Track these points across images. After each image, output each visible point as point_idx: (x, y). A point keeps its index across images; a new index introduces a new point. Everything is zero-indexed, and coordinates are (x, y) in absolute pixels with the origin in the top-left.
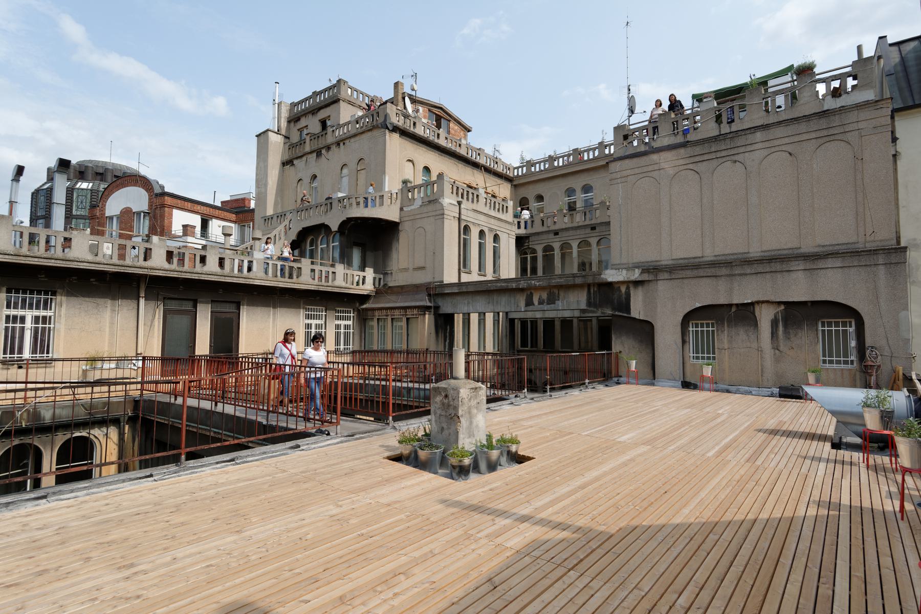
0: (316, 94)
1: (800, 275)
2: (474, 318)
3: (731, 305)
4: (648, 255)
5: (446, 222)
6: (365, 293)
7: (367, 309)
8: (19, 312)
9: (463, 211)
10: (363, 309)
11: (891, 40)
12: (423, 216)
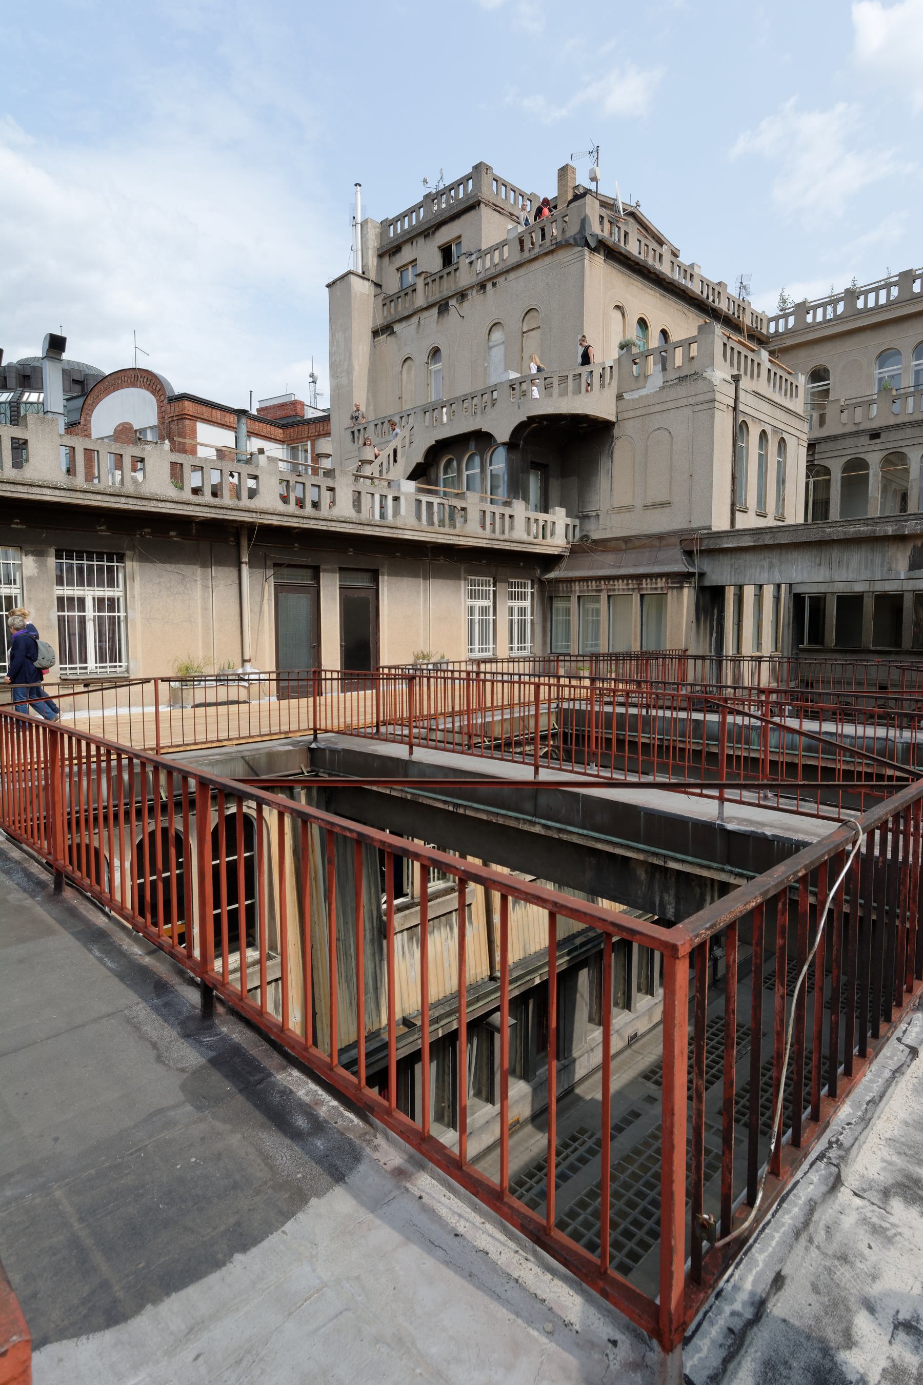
2: (749, 592)
5: (717, 413)
6: (555, 551)
7: (557, 581)
8: (75, 591)
9: (742, 394)
10: (550, 581)
12: (666, 406)
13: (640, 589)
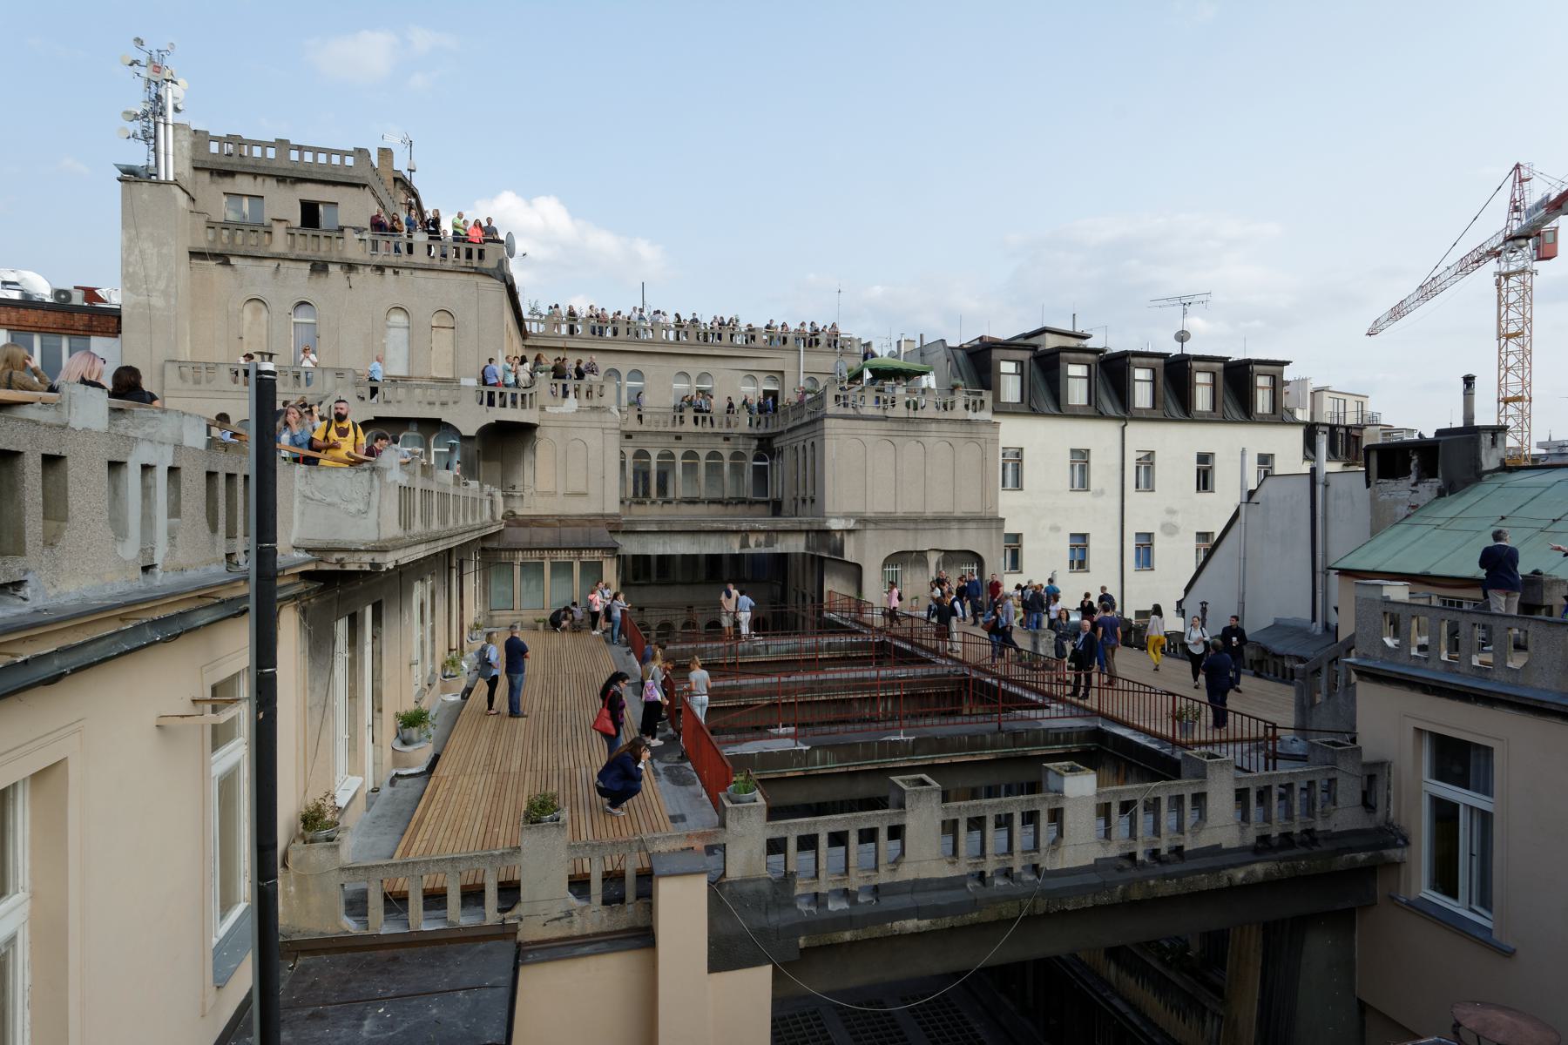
0: (282, 145)
1: (955, 532)
4: (857, 507)
11: (949, 344)
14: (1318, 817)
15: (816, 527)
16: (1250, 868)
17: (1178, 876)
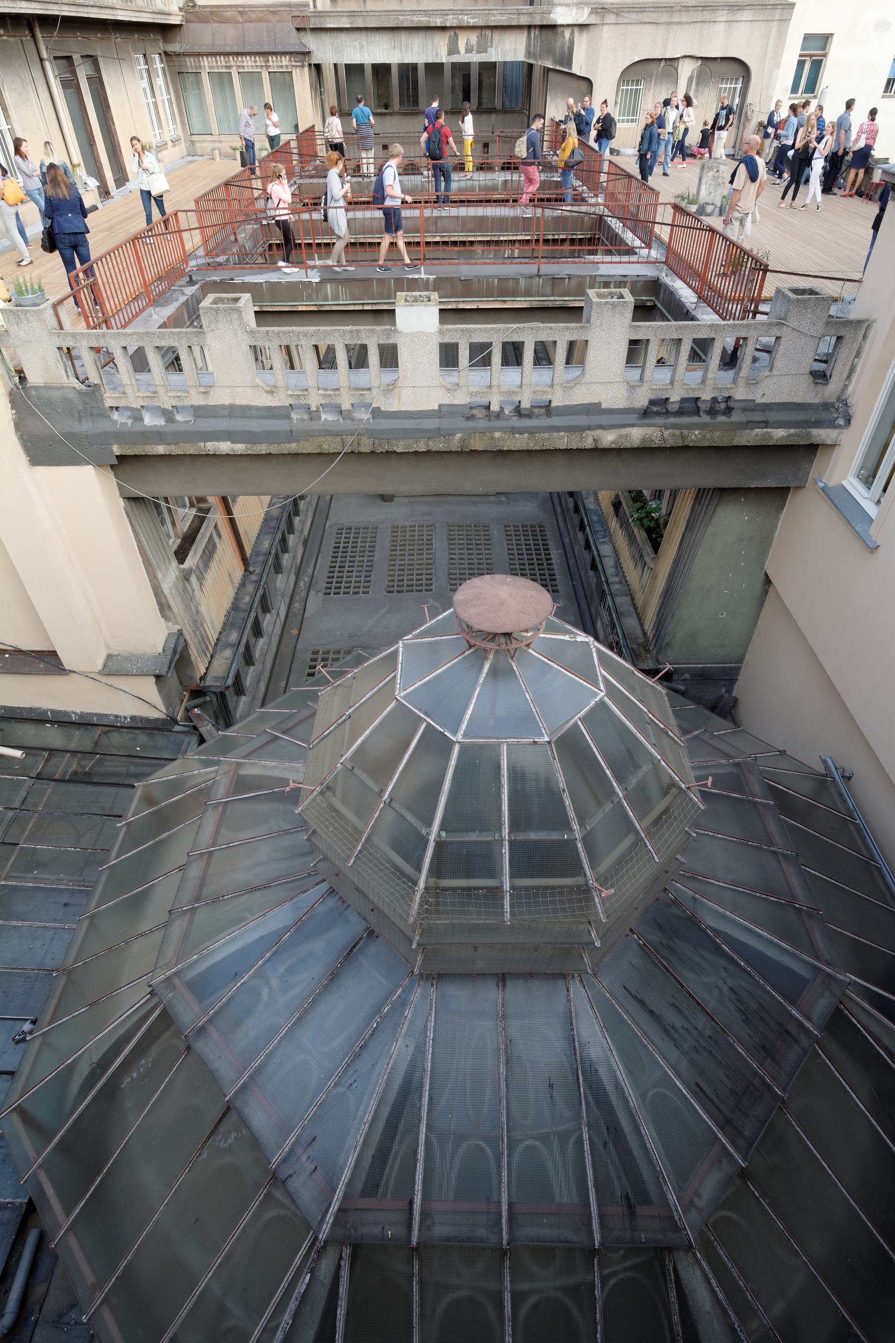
3: (660, 60)
13: (267, 67)
14: (741, 382)
15: (538, 22)
16: (624, 431)
17: (532, 431)
